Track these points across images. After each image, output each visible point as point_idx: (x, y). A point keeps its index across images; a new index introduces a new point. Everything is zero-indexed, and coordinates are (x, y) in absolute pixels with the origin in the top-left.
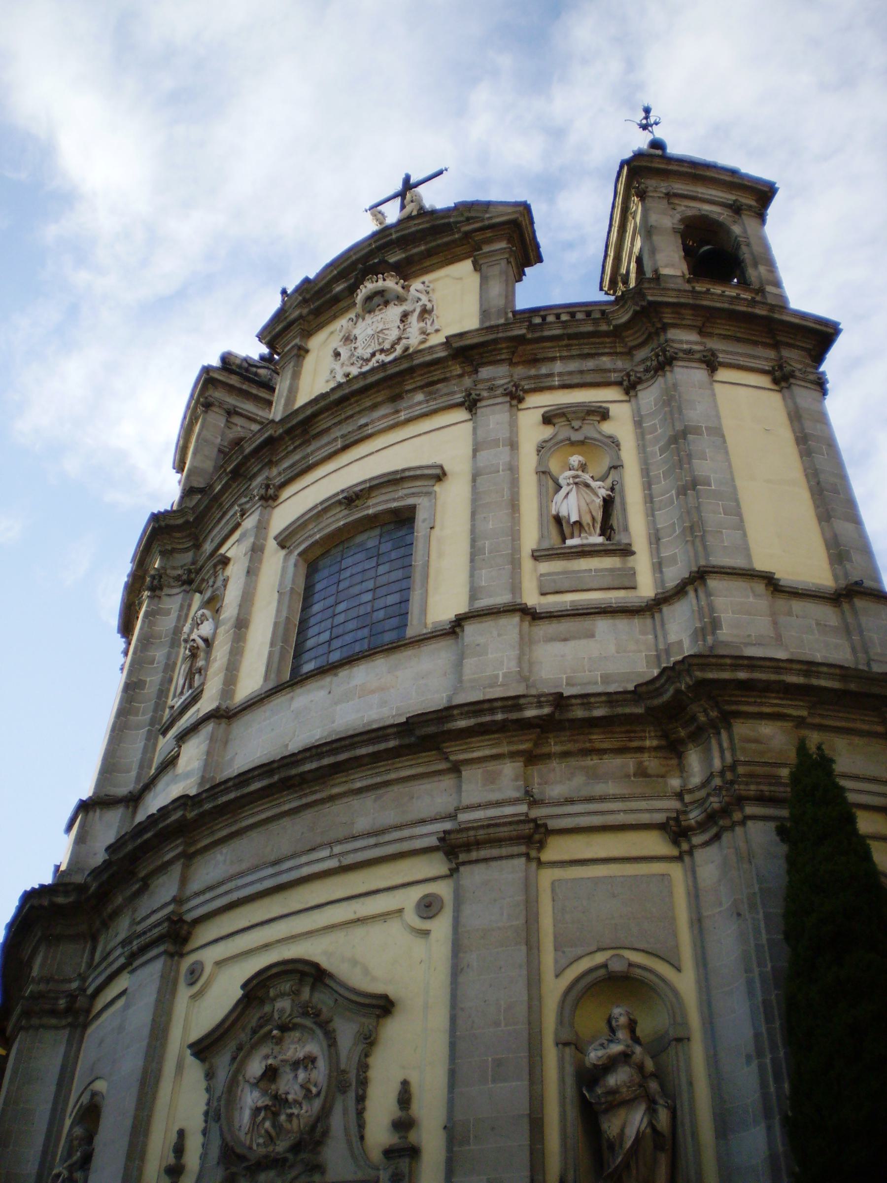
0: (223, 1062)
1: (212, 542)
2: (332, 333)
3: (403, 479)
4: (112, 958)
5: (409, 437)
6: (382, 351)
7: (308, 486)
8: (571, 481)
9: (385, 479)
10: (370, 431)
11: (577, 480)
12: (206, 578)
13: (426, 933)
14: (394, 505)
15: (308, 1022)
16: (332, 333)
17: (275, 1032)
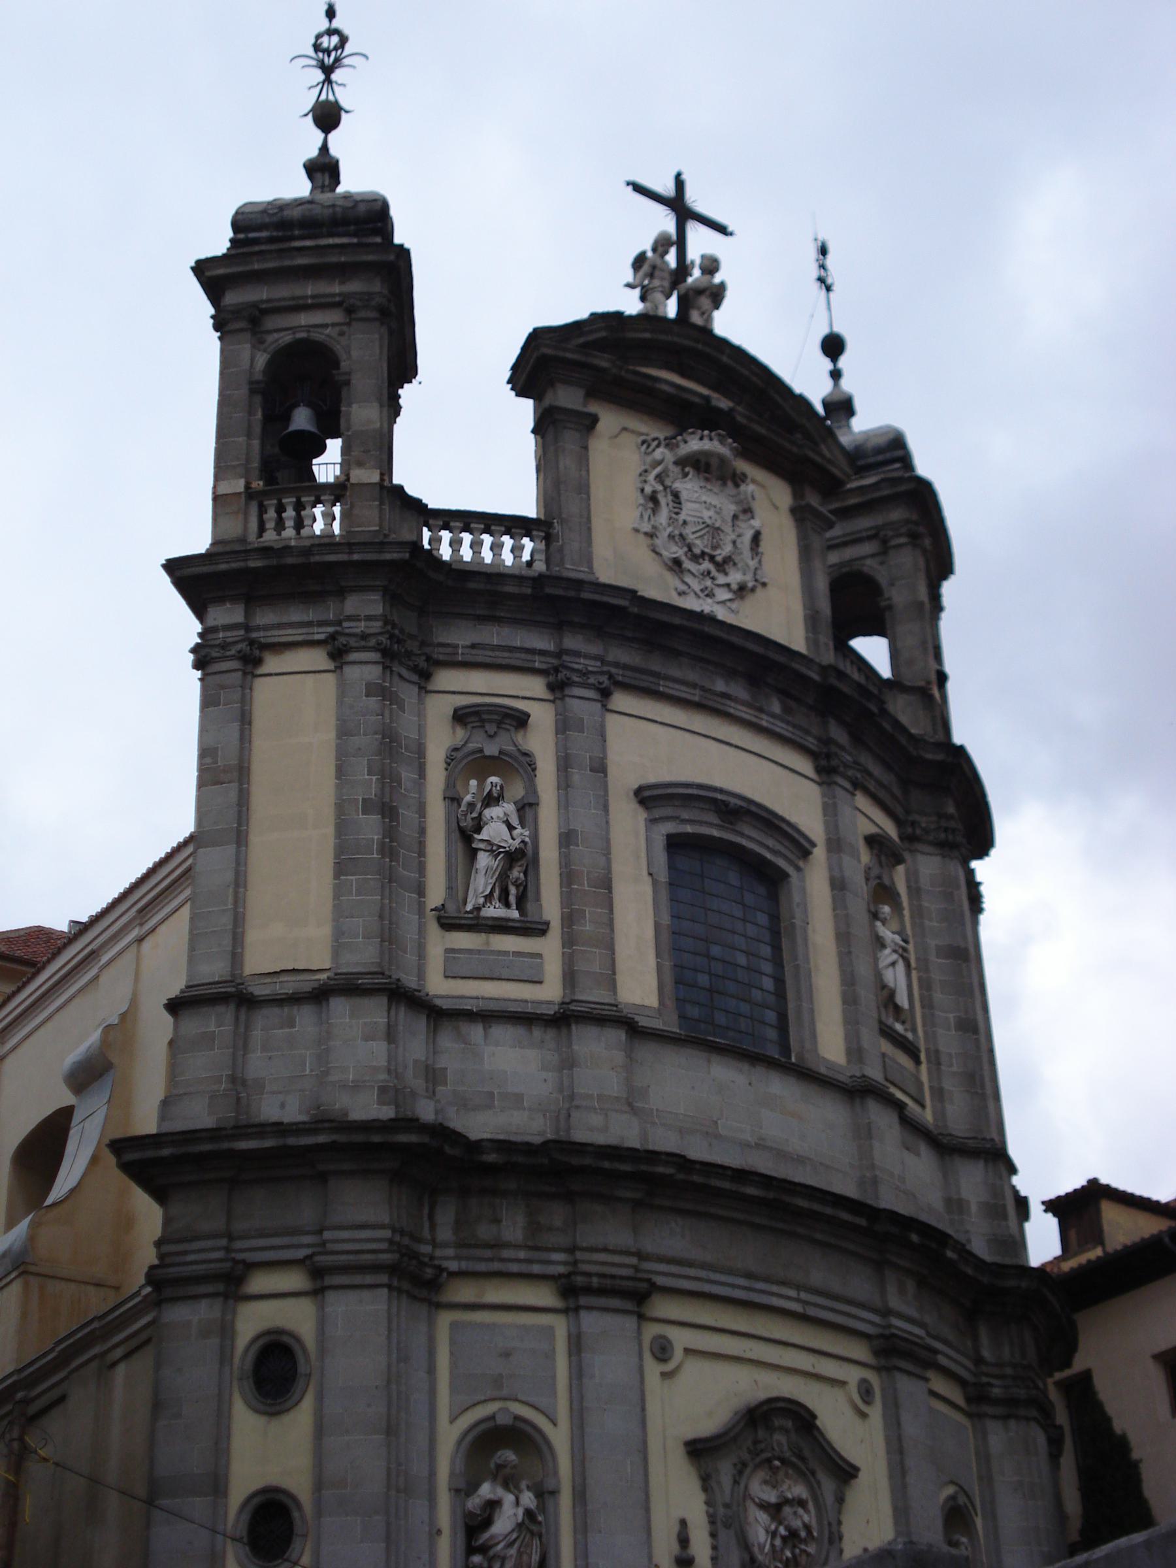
0: (725, 1470)
1: (473, 646)
2: (625, 429)
3: (778, 829)
4: (506, 1253)
5: (767, 756)
6: (712, 558)
7: (655, 722)
8: (900, 951)
9: (764, 814)
10: (732, 711)
11: (905, 954)
12: (485, 716)
13: (863, 1415)
14: (768, 856)
15: (800, 1464)
16: (625, 429)
17: (777, 1463)
